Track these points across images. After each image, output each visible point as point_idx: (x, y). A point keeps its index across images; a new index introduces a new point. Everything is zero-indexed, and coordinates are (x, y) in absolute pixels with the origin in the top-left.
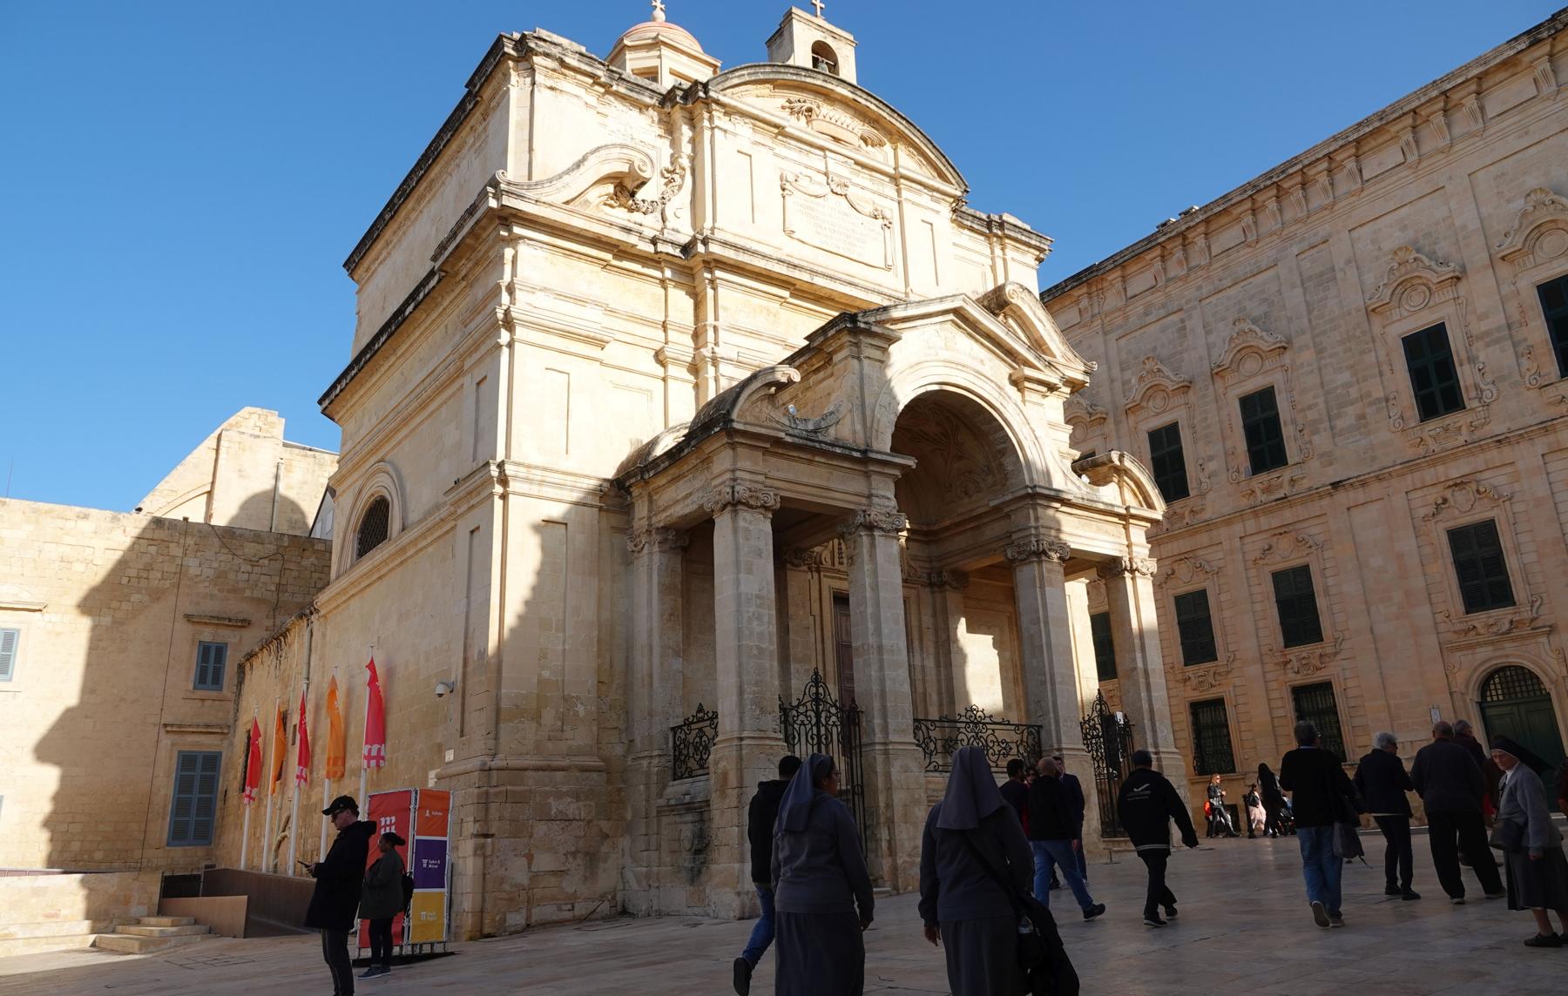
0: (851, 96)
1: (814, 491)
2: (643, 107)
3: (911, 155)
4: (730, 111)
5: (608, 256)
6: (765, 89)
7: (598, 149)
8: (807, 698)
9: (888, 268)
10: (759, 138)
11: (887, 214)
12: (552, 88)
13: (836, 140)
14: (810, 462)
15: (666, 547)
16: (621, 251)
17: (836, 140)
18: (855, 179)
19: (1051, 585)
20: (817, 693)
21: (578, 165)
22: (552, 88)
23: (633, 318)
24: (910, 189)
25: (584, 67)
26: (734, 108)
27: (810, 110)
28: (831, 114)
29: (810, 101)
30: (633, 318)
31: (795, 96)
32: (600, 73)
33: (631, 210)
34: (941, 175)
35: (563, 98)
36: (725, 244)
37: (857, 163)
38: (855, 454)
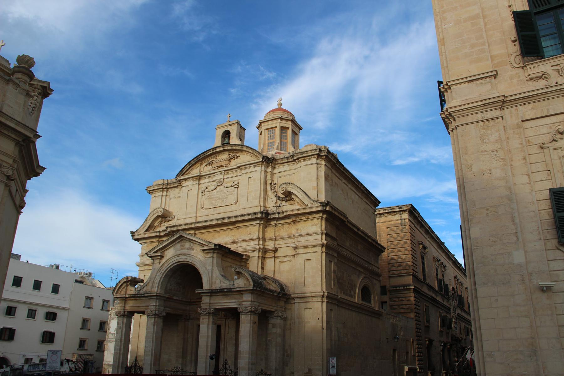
4: (185, 179)
9: (236, 203)
13: (220, 166)
17: (220, 166)
18: (226, 177)
21: (146, 220)
35: (157, 198)
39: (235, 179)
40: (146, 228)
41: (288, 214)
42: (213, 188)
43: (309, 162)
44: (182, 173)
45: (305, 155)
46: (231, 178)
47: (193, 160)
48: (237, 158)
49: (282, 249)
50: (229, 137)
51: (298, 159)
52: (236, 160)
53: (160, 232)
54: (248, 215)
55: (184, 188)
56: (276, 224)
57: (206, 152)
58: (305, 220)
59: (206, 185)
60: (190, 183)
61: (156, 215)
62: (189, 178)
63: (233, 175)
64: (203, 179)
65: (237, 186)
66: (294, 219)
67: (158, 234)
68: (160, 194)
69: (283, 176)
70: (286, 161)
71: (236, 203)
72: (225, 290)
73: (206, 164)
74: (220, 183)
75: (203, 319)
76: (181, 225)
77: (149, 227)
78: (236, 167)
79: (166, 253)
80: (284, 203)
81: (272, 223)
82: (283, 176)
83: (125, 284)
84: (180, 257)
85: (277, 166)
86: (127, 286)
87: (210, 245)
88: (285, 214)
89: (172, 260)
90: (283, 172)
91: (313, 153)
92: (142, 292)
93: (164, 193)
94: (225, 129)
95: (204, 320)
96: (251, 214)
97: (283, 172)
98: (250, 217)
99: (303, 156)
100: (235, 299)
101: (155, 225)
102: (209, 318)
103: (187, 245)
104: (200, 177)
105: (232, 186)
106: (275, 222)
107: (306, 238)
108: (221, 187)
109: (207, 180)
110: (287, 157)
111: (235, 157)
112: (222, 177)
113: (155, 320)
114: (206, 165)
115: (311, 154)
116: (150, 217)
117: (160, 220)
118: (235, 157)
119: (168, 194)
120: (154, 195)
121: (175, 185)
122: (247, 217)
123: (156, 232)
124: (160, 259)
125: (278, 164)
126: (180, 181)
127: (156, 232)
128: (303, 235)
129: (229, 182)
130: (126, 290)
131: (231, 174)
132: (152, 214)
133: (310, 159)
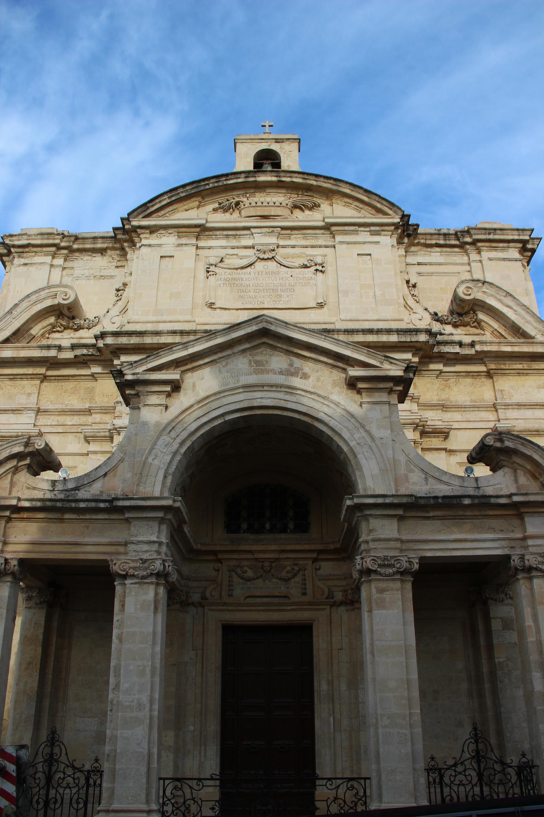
0: (274, 179)
1: (54, 548)
2: (102, 251)
3: (347, 205)
4: (153, 230)
5: (42, 371)
6: (194, 202)
7: (28, 296)
8: (40, 759)
9: (321, 306)
10: (184, 241)
11: (319, 260)
12: (25, 264)
14: (62, 520)
15: (32, 603)
16: (54, 363)
18: (282, 243)
19: (384, 608)
20: (51, 755)
22: (25, 264)
23: (63, 412)
24: (345, 233)
25: (45, 242)
26: (155, 226)
27: (237, 204)
28: (268, 199)
29: (233, 197)
30: (63, 412)
31: (222, 198)
32: (57, 241)
33: (76, 330)
34: (379, 211)
35: (32, 269)
36: (116, 334)
37: (283, 228)
38: (102, 505)
39: (309, 251)
40: (7, 333)
41: (486, 348)
42: (245, 262)
43: (501, 255)
44: (144, 209)
45: (496, 237)
46: (296, 249)
47: (184, 186)
48: (311, 209)
49: (459, 433)
50: (277, 165)
51: (474, 243)
52: (307, 212)
53: (60, 348)
54: (389, 331)
55: (144, 250)
56: (441, 372)
57: (227, 175)
58: (520, 373)
59: (222, 253)
60: (169, 240)
61: (48, 303)
62: (166, 227)
63: (304, 243)
64: (209, 237)
65: (320, 268)
66: (493, 366)
67: (53, 353)
68: (48, 259)
69: (431, 274)
70: (442, 242)
71: (321, 306)
72: (467, 501)
73: (216, 205)
74: (267, 256)
75: (382, 591)
76: (157, 333)
77: (15, 333)
78: (321, 224)
79: (190, 379)
80: (449, 329)
81: (432, 366)
82: (431, 274)
83: (14, 463)
84: (258, 395)
85: (413, 249)
86: (16, 470)
87: (386, 366)
88: (478, 348)
89: (225, 401)
90: (431, 264)
91: (516, 237)
92: (82, 494)
93: (59, 261)
94: (264, 146)
95: (387, 596)
96: (399, 332)
97: (431, 264)
98: (394, 338)
99: (491, 237)
100: (492, 530)
101: (34, 332)
102: (402, 589)
103: (278, 361)
104: (202, 230)
105: (305, 267)
106: (440, 366)
107: (529, 413)
108: (272, 265)
109: (223, 242)
110: (445, 235)
111: (310, 204)
112: (273, 240)
113: (156, 594)
114: (215, 210)
115: (510, 237)
116: (25, 304)
117: (52, 320)
118: (310, 204)
119: (69, 264)
120: (23, 261)
121: (99, 246)
122: (384, 338)
123: (49, 347)
124: (169, 395)
125: (418, 244)
126: (135, 229)
127: (49, 347)
128: (520, 406)
129: (299, 256)
130: (12, 484)
131: (296, 239)
132: (34, 298)
133: (503, 249)
